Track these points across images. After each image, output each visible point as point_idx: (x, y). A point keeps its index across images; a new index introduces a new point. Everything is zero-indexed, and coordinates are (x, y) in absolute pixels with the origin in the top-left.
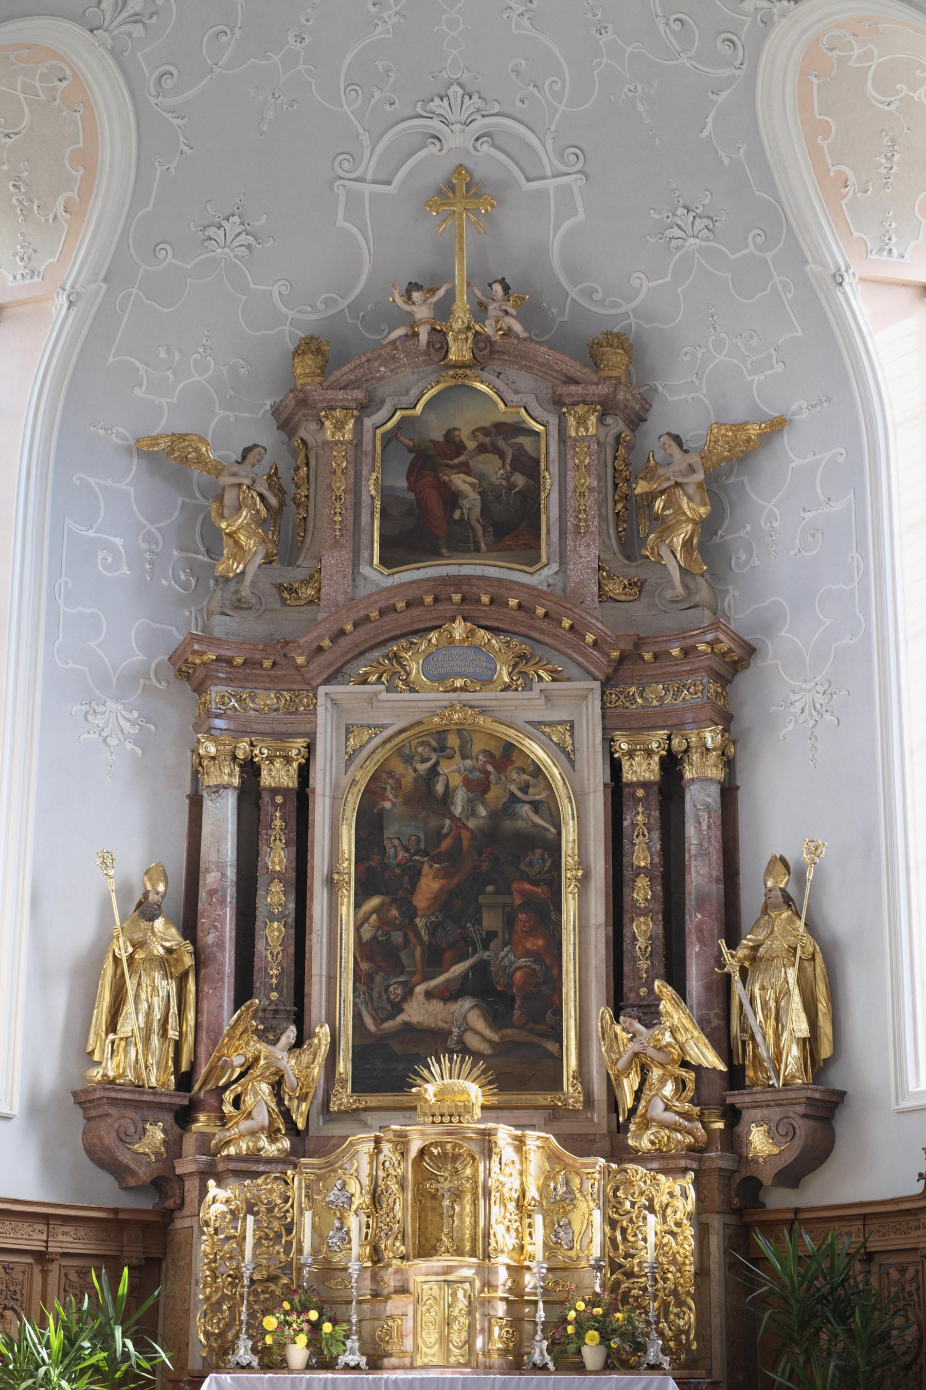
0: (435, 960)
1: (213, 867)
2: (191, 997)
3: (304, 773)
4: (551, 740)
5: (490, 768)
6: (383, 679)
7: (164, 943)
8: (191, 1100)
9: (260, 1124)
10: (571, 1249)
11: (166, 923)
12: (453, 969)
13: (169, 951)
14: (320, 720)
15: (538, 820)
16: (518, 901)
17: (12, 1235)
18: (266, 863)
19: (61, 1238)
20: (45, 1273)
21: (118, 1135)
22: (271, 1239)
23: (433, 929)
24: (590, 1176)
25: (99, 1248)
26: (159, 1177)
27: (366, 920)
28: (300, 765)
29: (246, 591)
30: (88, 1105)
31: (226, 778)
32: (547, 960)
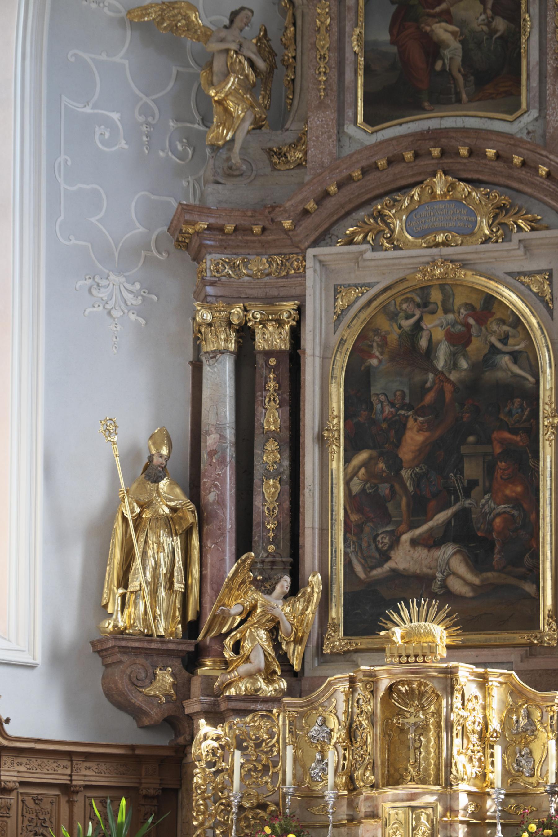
0: (419, 510)
1: (213, 429)
2: (196, 553)
3: (296, 335)
4: (531, 290)
5: (471, 321)
6: (368, 238)
7: (168, 503)
8: (197, 646)
9: (256, 667)
10: (532, 776)
11: (171, 484)
12: (436, 517)
13: (174, 510)
14: (309, 282)
15: (516, 370)
16: (498, 450)
17: (39, 771)
18: (262, 424)
19: (84, 772)
20: (71, 803)
21: (130, 680)
22: (259, 771)
23: (418, 480)
24: (549, 709)
25: (120, 780)
26: (169, 717)
27: (355, 473)
28: (292, 327)
29: (236, 159)
30: (104, 653)
31: (222, 343)
32: (525, 506)
